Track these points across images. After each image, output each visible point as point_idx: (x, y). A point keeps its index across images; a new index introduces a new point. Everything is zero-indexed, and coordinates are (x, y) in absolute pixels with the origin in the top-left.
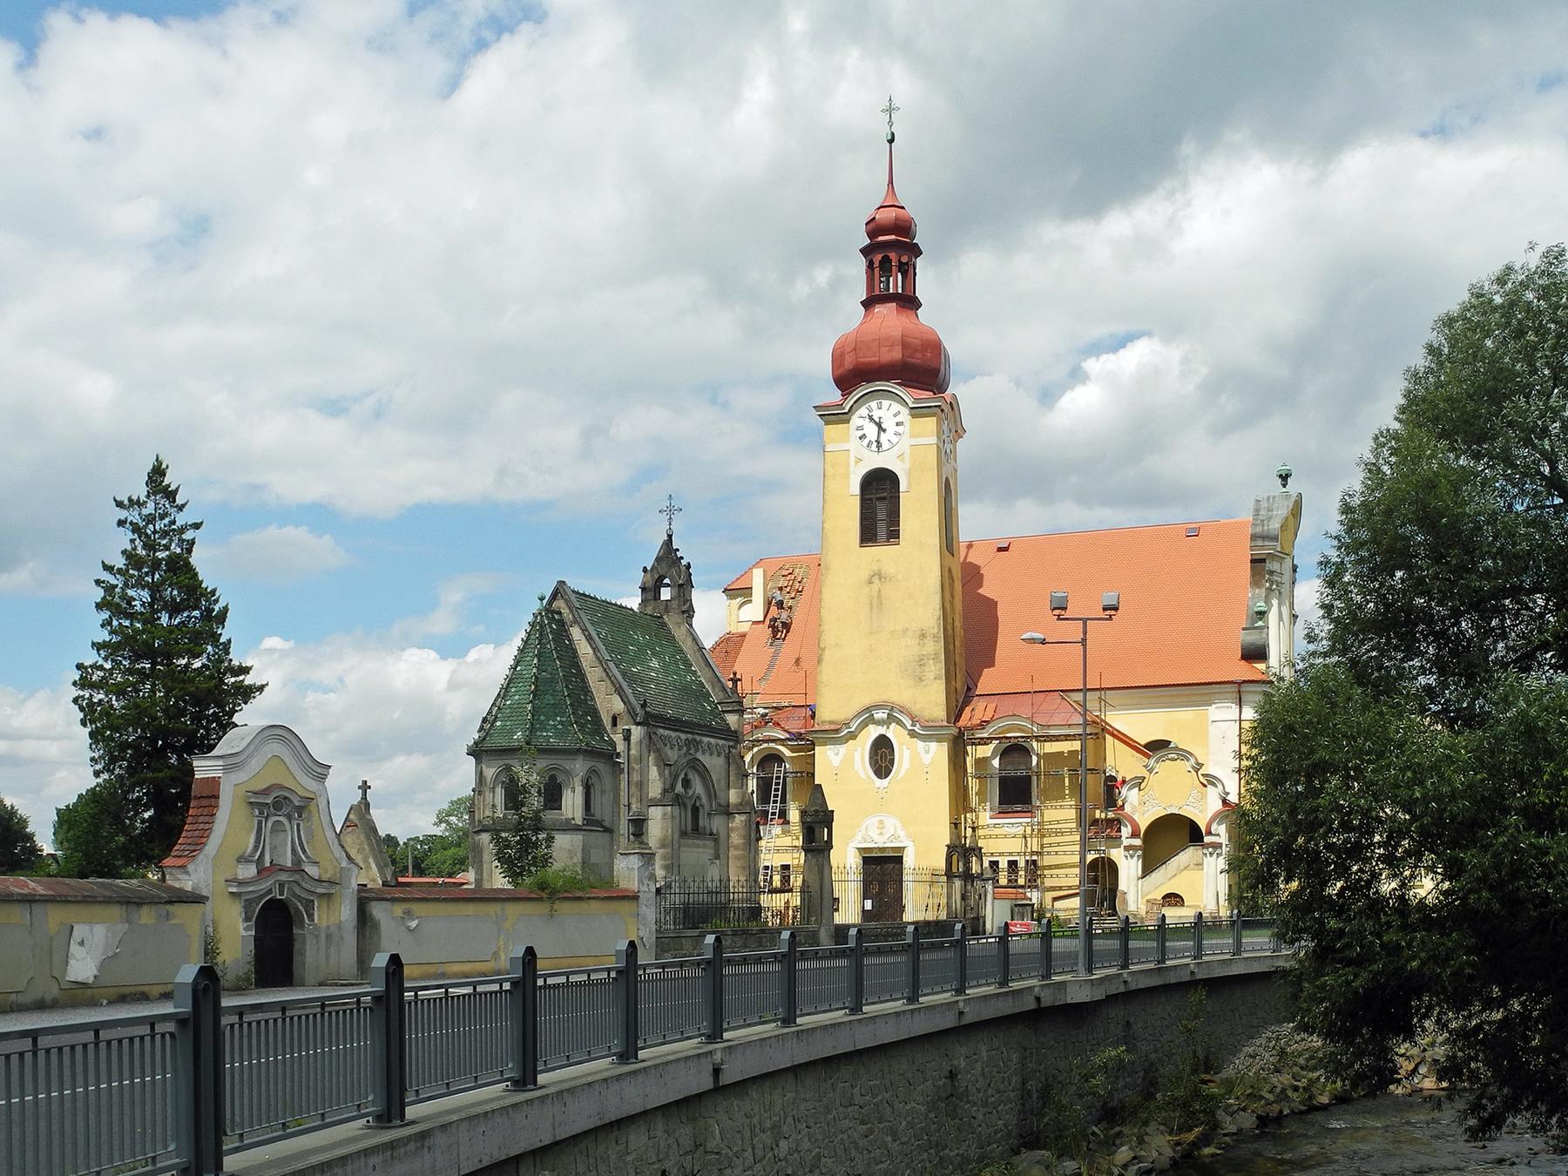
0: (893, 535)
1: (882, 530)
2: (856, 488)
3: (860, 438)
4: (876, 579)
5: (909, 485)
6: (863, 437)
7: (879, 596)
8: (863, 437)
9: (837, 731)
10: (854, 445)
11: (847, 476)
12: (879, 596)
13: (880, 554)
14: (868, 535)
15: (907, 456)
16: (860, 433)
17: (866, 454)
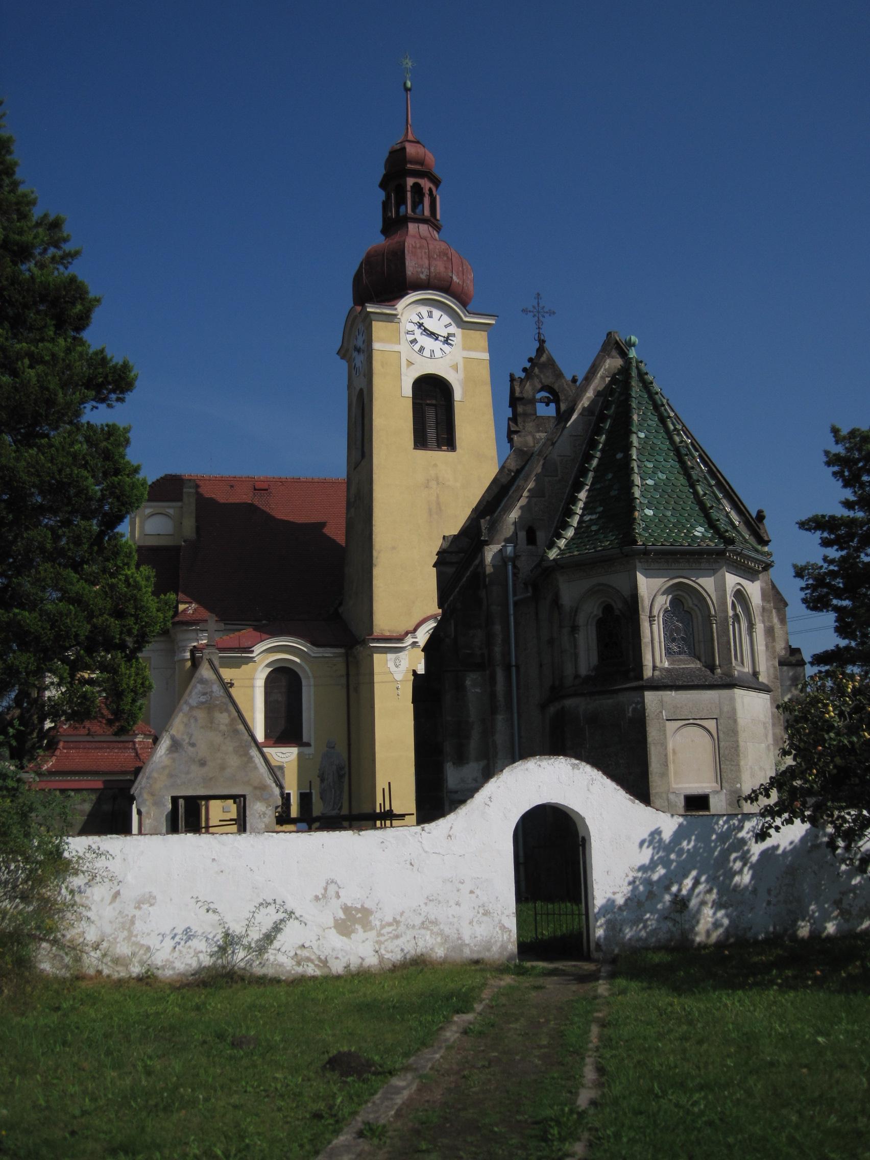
0: (447, 441)
1: (431, 433)
2: (408, 391)
3: (412, 342)
4: (433, 484)
5: (464, 393)
6: (414, 341)
7: (438, 504)
8: (414, 341)
9: (400, 639)
10: (404, 348)
11: (399, 377)
12: (438, 504)
13: (439, 457)
14: (421, 441)
15: (461, 367)
16: (410, 337)
17: (416, 358)
